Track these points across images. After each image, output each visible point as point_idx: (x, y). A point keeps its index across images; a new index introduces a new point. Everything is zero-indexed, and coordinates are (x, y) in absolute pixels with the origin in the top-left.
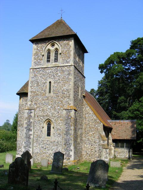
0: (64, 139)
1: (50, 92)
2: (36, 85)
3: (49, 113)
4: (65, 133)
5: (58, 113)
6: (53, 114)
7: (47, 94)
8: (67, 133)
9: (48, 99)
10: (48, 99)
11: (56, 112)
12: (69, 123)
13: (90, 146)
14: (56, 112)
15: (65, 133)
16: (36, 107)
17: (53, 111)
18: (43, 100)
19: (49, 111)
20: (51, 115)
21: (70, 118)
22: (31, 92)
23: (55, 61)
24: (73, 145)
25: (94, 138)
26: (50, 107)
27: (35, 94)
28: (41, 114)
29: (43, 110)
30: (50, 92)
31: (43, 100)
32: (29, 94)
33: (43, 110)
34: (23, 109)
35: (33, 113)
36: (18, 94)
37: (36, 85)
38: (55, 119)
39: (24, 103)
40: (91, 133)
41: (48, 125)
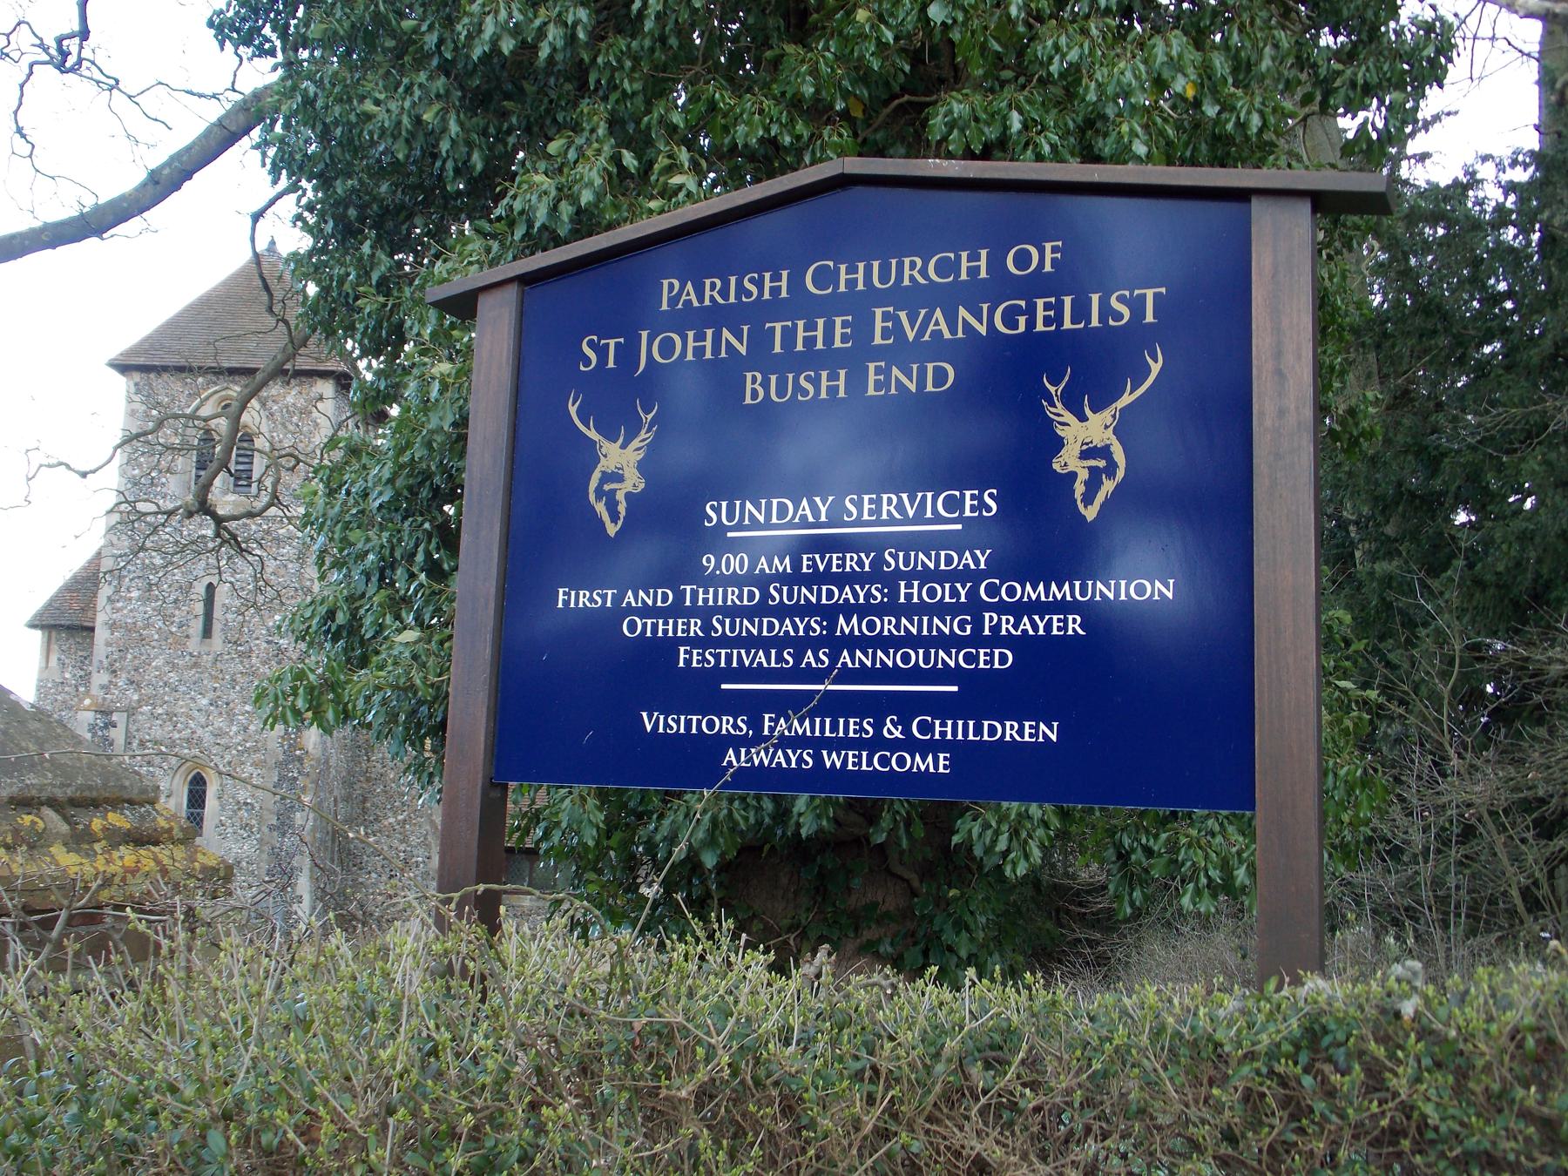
0: (267, 848)
1: (207, 632)
2: (135, 594)
3: (200, 732)
4: (274, 822)
5: (246, 729)
6: (218, 734)
7: (194, 645)
8: (283, 825)
9: (196, 665)
10: (196, 665)
11: (234, 729)
12: (295, 779)
13: (384, 878)
14: (234, 729)
15: (274, 822)
16: (136, 697)
17: (220, 723)
18: (174, 667)
19: (203, 720)
20: (208, 738)
21: (300, 759)
22: (113, 626)
23: (236, 485)
24: (306, 871)
25: (402, 841)
26: (205, 702)
27: (132, 637)
28: (157, 732)
29: (171, 715)
30: (207, 632)
31: (174, 667)
32: (101, 634)
33: (171, 715)
34: (64, 702)
35: (121, 727)
36: (32, 626)
37: (135, 594)
38: (228, 758)
39: (67, 675)
40: (392, 820)
41: (191, 783)
